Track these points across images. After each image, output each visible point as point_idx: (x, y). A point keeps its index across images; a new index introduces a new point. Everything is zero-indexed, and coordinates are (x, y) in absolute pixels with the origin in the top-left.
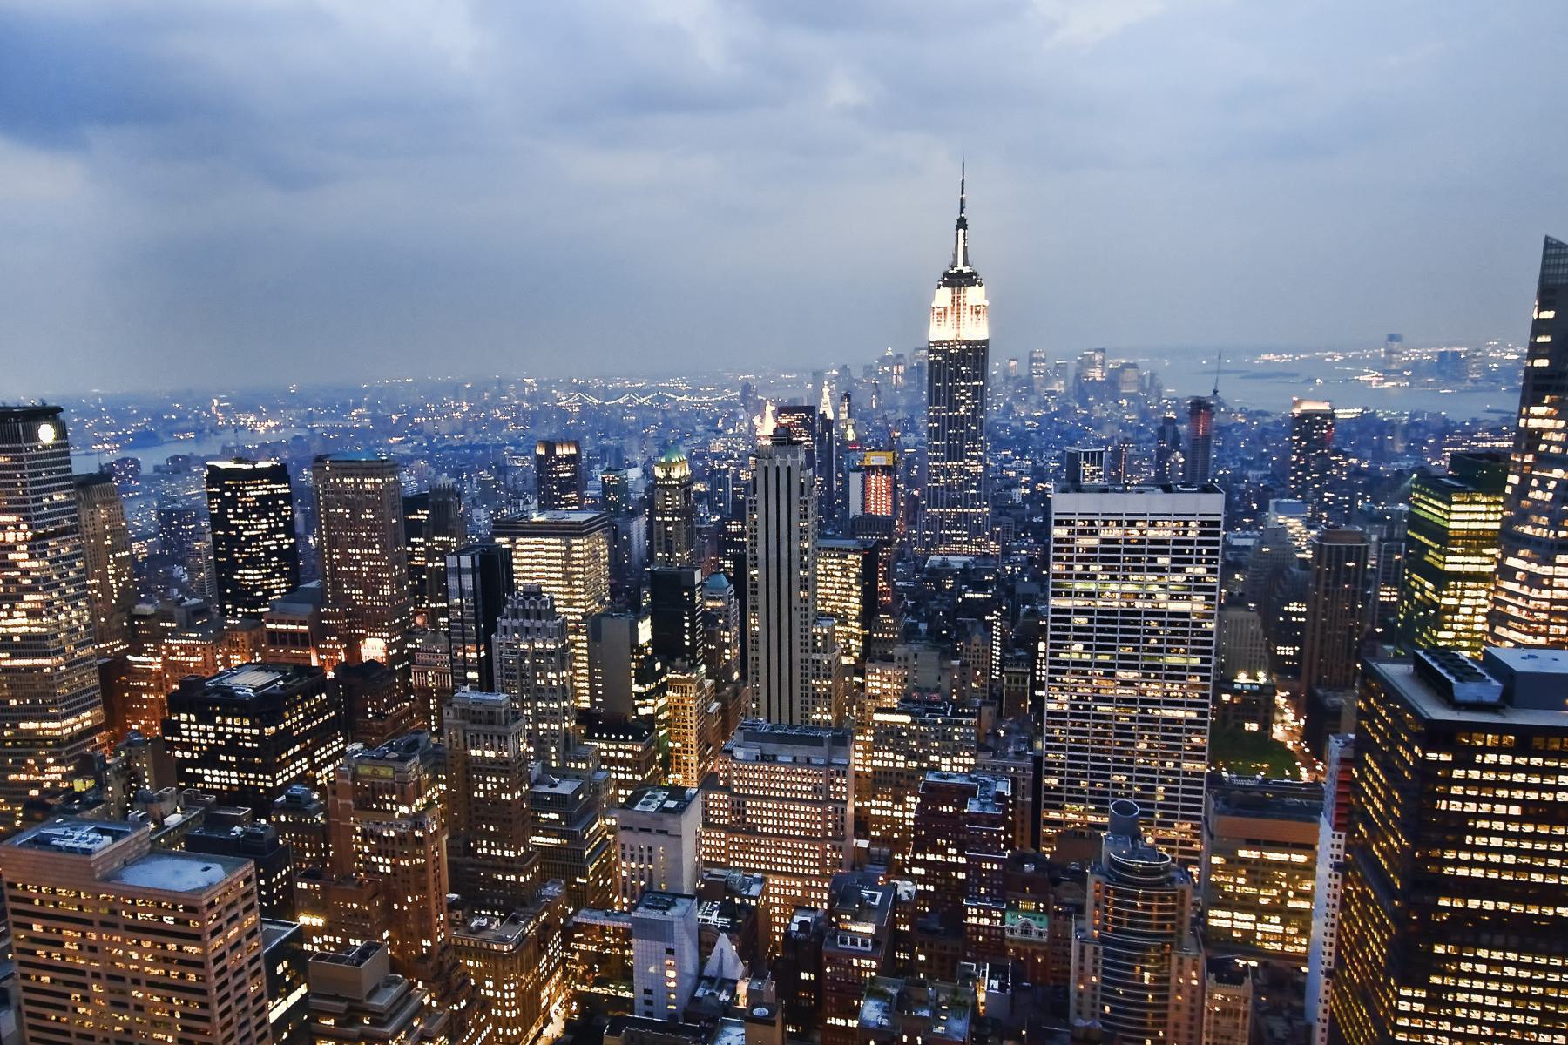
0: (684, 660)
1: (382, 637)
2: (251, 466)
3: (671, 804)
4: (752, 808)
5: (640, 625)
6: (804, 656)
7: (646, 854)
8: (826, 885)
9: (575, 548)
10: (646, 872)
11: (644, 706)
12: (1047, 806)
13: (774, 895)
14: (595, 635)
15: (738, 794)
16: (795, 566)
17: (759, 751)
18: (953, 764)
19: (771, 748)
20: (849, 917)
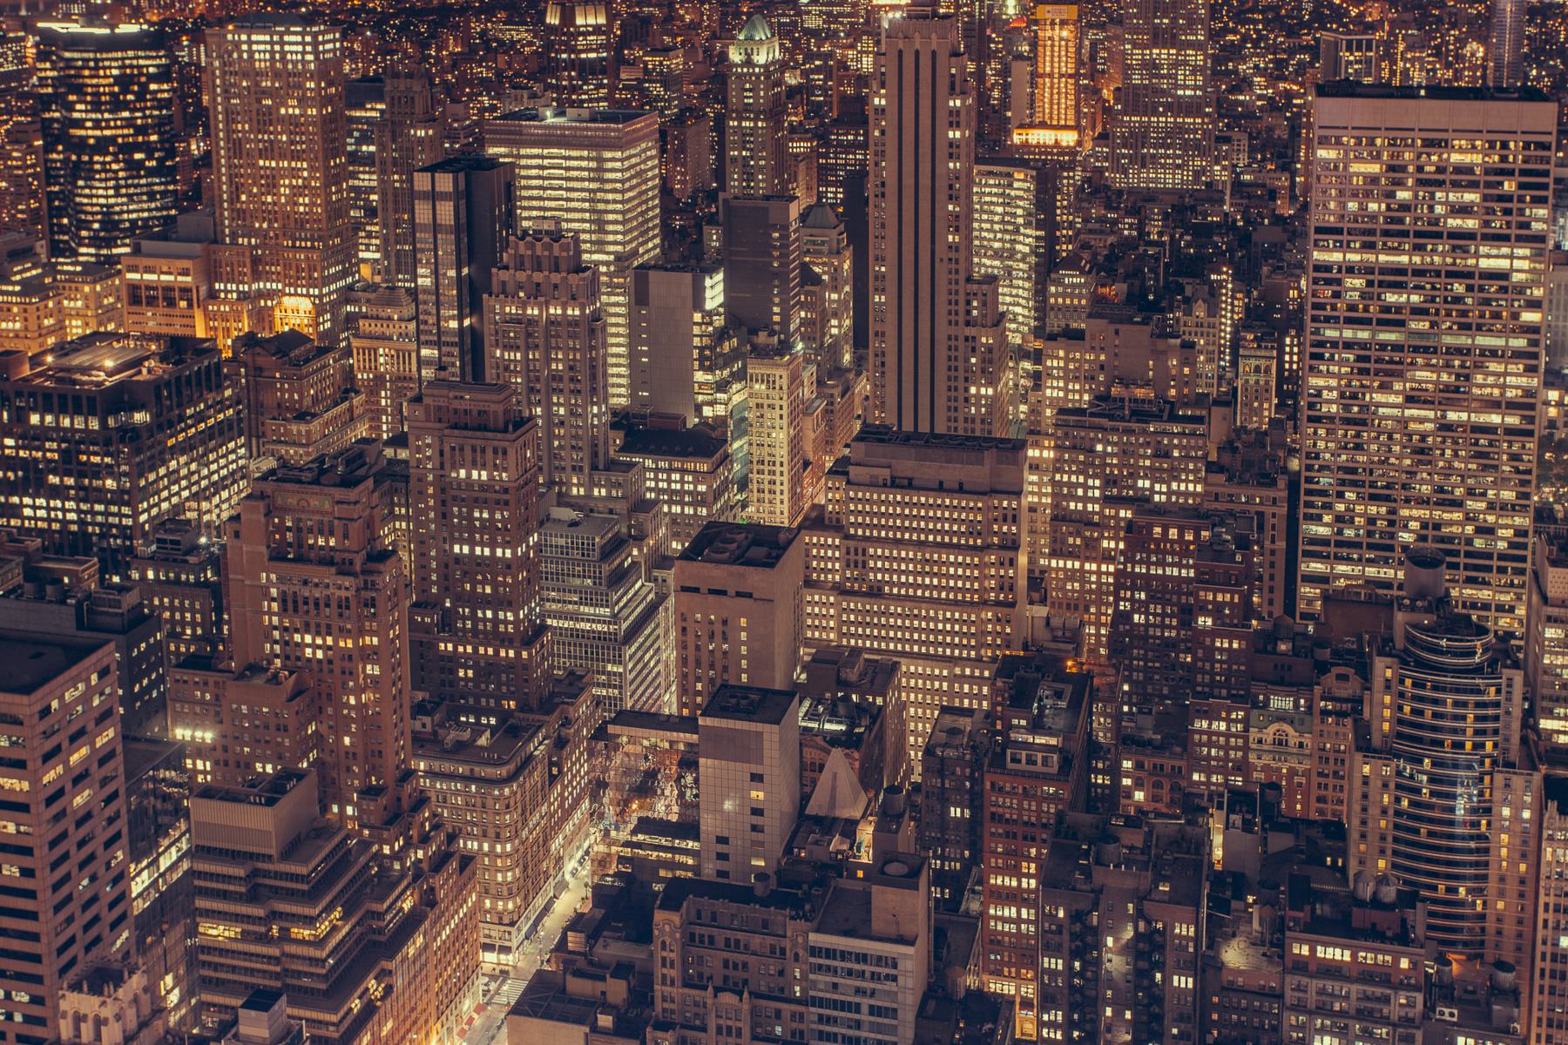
0: (772, 333)
1: (308, 296)
2: (107, 31)
3: (758, 552)
4: (876, 558)
5: (708, 282)
6: (953, 331)
7: (718, 628)
8: (987, 674)
9: (610, 165)
10: (718, 655)
11: (712, 404)
12: (1307, 554)
13: (909, 689)
14: (640, 297)
15: (854, 537)
16: (941, 195)
17: (886, 473)
18: (1170, 493)
19: (907, 465)
20: (1023, 722)
